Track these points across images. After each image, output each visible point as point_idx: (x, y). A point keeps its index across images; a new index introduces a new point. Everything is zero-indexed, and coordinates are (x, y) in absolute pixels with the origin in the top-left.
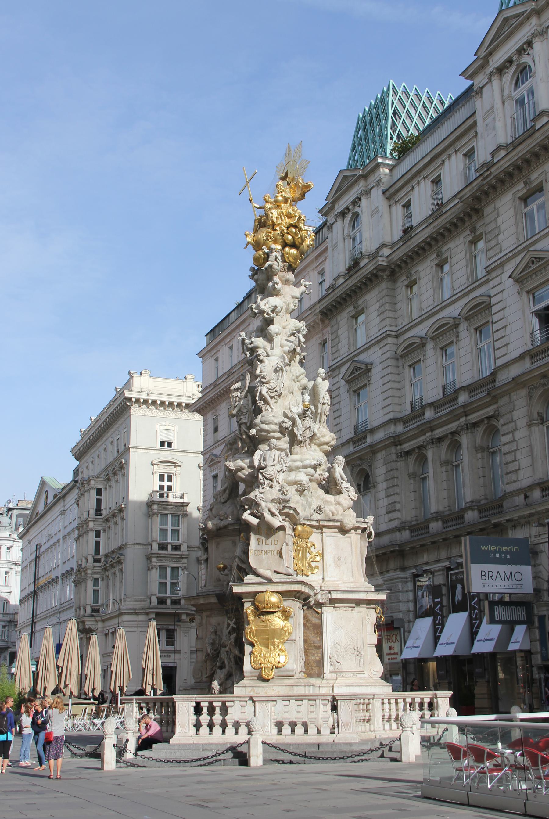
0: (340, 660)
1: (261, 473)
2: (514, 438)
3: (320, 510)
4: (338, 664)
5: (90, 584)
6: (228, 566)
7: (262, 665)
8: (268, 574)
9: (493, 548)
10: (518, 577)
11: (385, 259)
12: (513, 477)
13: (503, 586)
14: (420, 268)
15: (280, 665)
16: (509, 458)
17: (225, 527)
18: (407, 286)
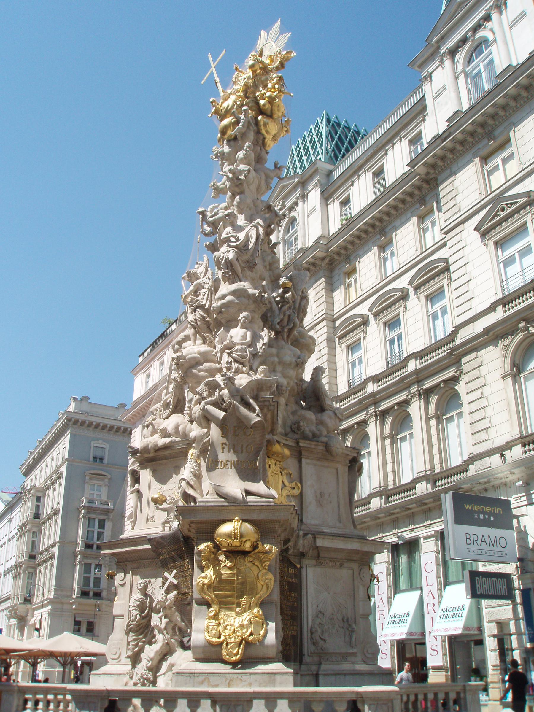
0: (326, 636)
1: (229, 354)
2: (482, 394)
3: (299, 428)
4: (321, 643)
6: (168, 498)
9: (476, 508)
11: (323, 246)
12: (483, 436)
17: (166, 447)
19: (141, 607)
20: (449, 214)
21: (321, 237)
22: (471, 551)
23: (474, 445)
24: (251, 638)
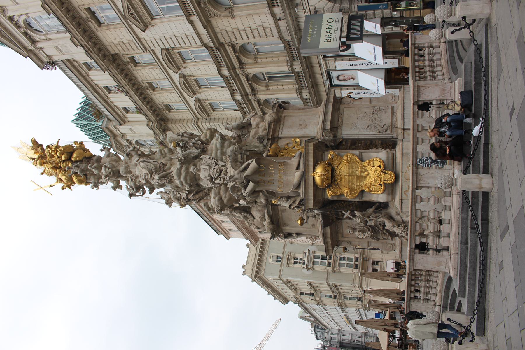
0: (382, 124)
1: (215, 179)
2: (243, 30)
4: (385, 126)
5: (347, 301)
7: (382, 183)
8: (298, 174)
9: (310, 35)
10: (330, 21)
12: (268, 30)
13: (336, 29)
14: (157, 102)
15: (382, 166)
16: (256, 34)
17: (270, 217)
18: (170, 112)
19: (363, 232)
20: (134, 48)
21: (148, 125)
22: (335, 39)
23: (273, 36)
24: (382, 166)
